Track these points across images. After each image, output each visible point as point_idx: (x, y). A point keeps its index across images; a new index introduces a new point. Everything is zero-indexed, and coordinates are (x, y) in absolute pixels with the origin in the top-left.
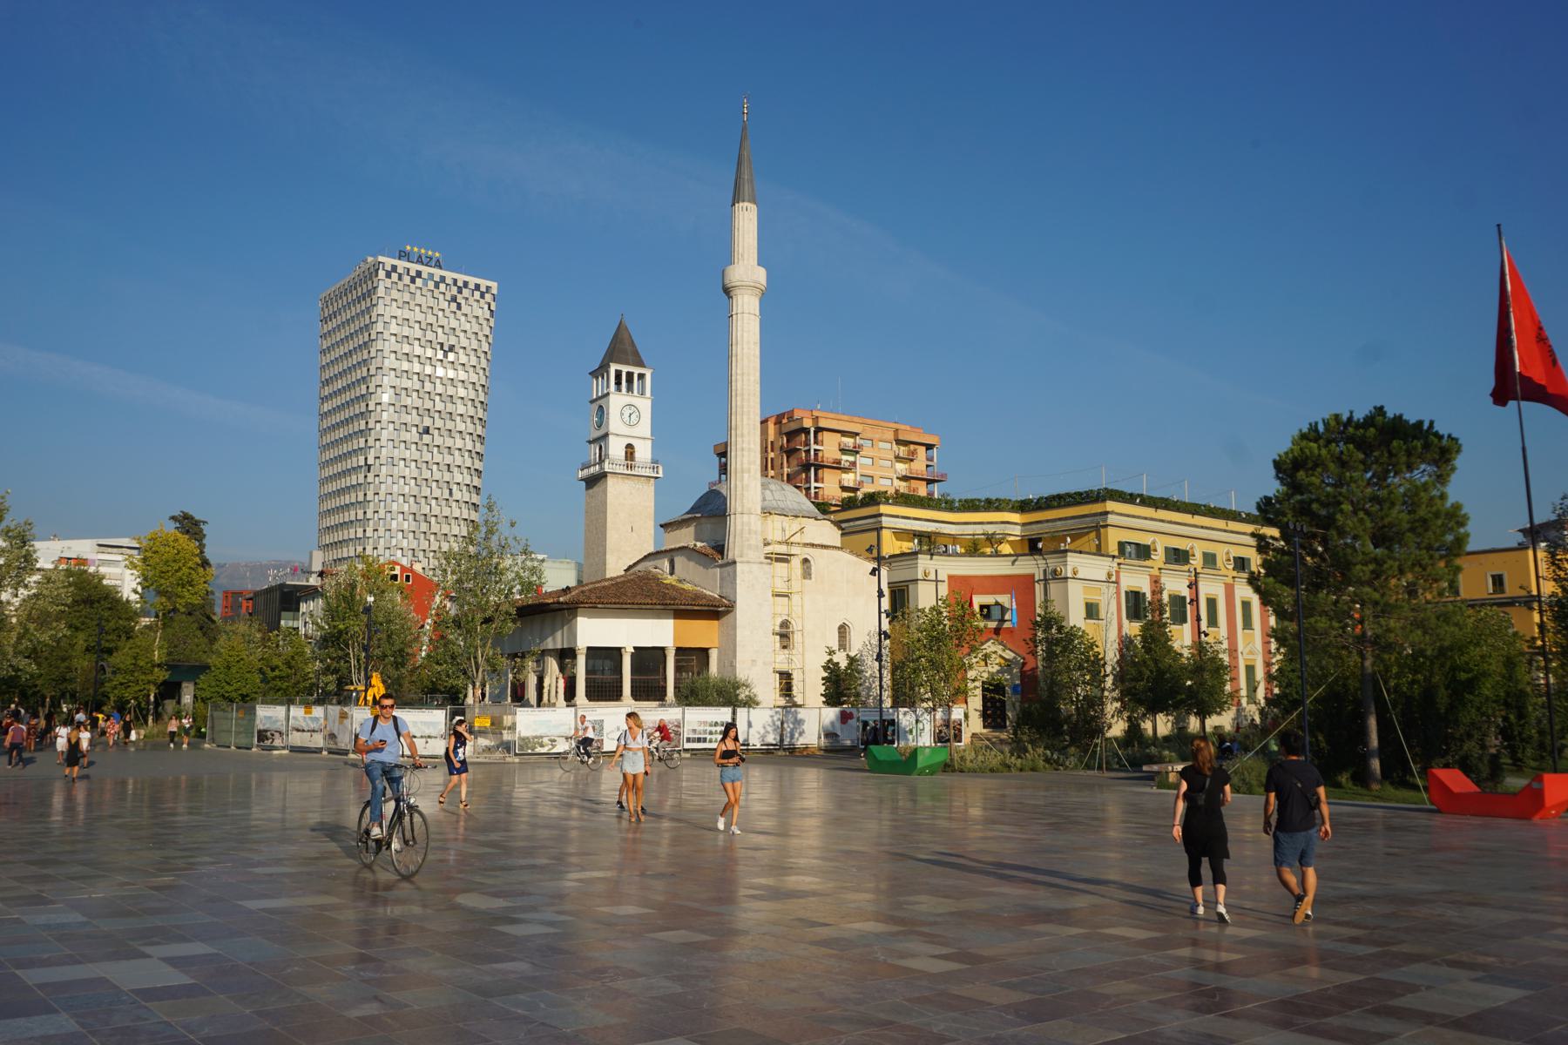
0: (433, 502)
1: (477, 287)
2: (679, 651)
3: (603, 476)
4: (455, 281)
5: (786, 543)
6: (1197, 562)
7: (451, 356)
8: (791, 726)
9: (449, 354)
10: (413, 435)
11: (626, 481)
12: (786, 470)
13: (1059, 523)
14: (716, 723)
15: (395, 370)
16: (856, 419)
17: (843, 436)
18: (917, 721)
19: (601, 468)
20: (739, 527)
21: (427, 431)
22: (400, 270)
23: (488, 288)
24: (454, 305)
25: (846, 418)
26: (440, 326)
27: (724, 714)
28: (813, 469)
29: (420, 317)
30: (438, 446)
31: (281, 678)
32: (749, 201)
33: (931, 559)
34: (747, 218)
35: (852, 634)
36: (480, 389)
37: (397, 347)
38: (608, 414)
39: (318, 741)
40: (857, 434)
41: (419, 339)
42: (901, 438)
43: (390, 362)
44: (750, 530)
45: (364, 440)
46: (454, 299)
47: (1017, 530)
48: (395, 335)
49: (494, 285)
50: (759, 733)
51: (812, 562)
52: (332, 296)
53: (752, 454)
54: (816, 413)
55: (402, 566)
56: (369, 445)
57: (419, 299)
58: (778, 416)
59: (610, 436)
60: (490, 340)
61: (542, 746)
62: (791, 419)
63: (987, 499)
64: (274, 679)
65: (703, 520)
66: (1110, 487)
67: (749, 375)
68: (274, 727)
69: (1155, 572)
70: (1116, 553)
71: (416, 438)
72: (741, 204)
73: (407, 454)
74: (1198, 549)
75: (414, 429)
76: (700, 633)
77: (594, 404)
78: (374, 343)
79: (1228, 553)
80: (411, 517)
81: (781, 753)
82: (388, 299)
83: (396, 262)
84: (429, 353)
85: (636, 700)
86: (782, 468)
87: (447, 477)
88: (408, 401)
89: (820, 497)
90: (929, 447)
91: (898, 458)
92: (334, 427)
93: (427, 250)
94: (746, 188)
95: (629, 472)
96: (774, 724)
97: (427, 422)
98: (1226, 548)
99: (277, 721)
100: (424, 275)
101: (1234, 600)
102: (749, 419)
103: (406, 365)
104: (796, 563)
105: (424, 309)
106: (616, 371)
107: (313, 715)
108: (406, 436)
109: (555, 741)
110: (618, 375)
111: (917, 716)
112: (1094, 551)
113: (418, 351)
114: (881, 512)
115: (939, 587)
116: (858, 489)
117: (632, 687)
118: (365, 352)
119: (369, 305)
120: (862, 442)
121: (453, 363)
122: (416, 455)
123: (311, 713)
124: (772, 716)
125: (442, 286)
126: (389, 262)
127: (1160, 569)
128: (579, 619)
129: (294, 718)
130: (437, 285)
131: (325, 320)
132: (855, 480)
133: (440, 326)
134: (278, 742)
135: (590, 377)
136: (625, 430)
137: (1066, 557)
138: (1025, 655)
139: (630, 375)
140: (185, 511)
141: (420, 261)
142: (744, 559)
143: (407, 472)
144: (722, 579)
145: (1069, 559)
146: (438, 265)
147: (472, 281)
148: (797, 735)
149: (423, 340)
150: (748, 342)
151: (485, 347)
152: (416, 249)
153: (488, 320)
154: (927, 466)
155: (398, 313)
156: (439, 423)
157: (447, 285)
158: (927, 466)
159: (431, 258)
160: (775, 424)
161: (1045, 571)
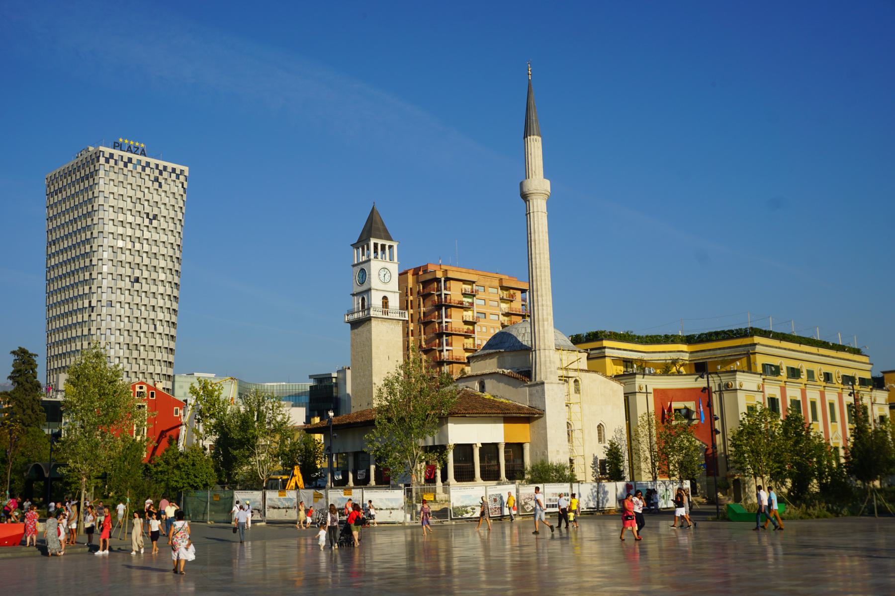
0: (142, 335)
1: (174, 170)
2: (508, 445)
3: (368, 319)
4: (157, 166)
5: (566, 369)
6: (804, 376)
12: (422, 309)
13: (719, 351)
15: (113, 233)
16: (471, 271)
17: (464, 284)
18: (666, 490)
19: (369, 314)
21: (137, 280)
22: (116, 157)
23: (182, 171)
24: (156, 184)
25: (464, 270)
27: (565, 488)
28: (444, 308)
29: (131, 193)
30: (146, 292)
31: (161, 472)
32: (537, 135)
33: (643, 378)
34: (535, 145)
35: (605, 431)
36: (176, 248)
37: (113, 216)
38: (370, 275)
40: (474, 282)
41: (131, 210)
42: (504, 284)
43: (110, 228)
44: (550, 360)
45: (88, 287)
46: (157, 179)
47: (686, 357)
48: (113, 207)
49: (186, 169)
51: (580, 382)
53: (549, 308)
54: (444, 267)
55: (148, 386)
56: (93, 291)
57: (131, 179)
58: (415, 269)
59: (372, 291)
60: (184, 211)
61: (467, 513)
62: (425, 272)
63: (666, 335)
64: (156, 473)
65: (505, 354)
66: (754, 327)
67: (544, 253)
69: (782, 384)
70: (761, 372)
71: (129, 285)
72: (532, 137)
73: (122, 298)
74: (805, 367)
75: (128, 279)
76: (521, 433)
77: (355, 268)
78: (96, 213)
79: (820, 370)
80: (125, 347)
81: (598, 514)
84: (139, 220)
85: (484, 481)
86: (419, 307)
88: (122, 258)
89: (449, 328)
90: (523, 291)
91: (502, 300)
93: (135, 142)
94: (534, 126)
95: (386, 317)
97: (137, 273)
98: (819, 366)
99: (256, 502)
100: (134, 161)
101: (825, 401)
102: (545, 284)
103: (121, 230)
104: (571, 381)
105: (134, 187)
106: (374, 243)
107: (287, 497)
108: (121, 284)
109: (474, 509)
110: (376, 245)
111: (666, 486)
112: (746, 369)
113: (130, 219)
114: (604, 346)
116: (475, 323)
117: (481, 471)
118: (89, 220)
119: (91, 183)
120: (477, 288)
121: (156, 228)
122: (129, 299)
123: (285, 495)
124: (592, 490)
125: (148, 169)
126: (108, 151)
127: (785, 382)
129: (270, 499)
130: (144, 169)
131: (50, 195)
132: (473, 317)
133: (146, 200)
135: (352, 247)
136: (381, 286)
137: (735, 375)
138: (707, 443)
139: (383, 247)
140: (23, 347)
141: (129, 150)
143: (122, 312)
144: (531, 395)
145: (737, 376)
146: (143, 153)
147: (170, 165)
148: (605, 501)
149: (134, 211)
151: (180, 216)
152: (126, 141)
153: (182, 195)
154: (522, 305)
155: (115, 190)
156: (146, 274)
157: (151, 168)
158: (522, 305)
159: (138, 148)
160: (413, 275)
161: (719, 385)
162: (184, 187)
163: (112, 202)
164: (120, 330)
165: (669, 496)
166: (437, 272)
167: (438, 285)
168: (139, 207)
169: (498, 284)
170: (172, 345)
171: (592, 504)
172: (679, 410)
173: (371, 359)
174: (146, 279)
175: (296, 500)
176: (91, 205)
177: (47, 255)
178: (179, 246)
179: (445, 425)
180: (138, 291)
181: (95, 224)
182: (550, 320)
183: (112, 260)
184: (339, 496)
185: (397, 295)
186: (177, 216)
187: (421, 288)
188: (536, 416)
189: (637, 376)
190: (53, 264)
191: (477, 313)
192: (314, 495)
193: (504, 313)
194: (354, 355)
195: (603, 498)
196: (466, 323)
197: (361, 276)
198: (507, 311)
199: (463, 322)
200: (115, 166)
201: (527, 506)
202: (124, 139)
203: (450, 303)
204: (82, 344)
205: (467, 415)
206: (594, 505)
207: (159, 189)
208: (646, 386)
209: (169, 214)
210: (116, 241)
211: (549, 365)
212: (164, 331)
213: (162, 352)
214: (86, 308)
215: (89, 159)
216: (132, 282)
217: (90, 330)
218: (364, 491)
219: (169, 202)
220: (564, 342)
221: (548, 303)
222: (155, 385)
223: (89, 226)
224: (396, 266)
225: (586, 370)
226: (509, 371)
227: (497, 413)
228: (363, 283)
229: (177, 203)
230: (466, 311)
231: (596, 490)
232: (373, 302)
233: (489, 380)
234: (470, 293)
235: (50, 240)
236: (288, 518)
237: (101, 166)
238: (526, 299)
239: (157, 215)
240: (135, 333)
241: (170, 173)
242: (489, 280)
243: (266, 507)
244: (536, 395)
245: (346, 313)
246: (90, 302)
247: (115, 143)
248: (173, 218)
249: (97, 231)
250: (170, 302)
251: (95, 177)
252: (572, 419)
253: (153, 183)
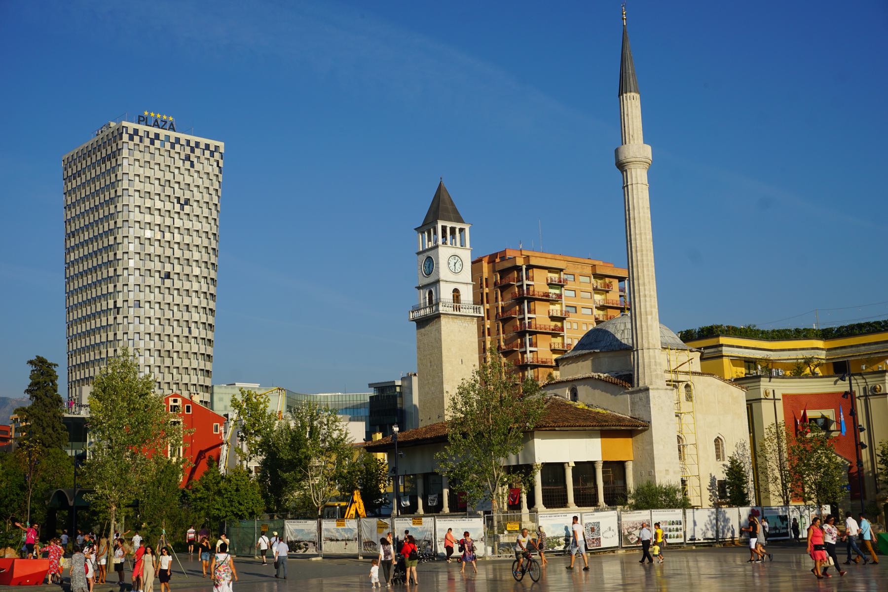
0: (175, 340)
1: (207, 147)
2: (606, 463)
3: (438, 316)
4: (188, 142)
5: (675, 372)
7: (187, 209)
8: (722, 524)
9: (185, 206)
10: (156, 280)
11: (455, 321)
13: (863, 348)
14: (673, 522)
15: (139, 222)
16: (558, 257)
17: (550, 272)
19: (437, 310)
20: (646, 361)
21: (168, 276)
22: (141, 133)
23: (217, 147)
24: (188, 164)
25: (549, 256)
26: (176, 182)
28: (526, 302)
29: (159, 174)
30: (178, 289)
31: (200, 498)
32: (636, 92)
33: (770, 381)
34: (633, 105)
35: (724, 446)
36: (212, 237)
37: (139, 202)
38: (438, 264)
39: (353, 548)
40: (561, 270)
41: (159, 195)
42: (598, 272)
43: (136, 215)
44: (655, 362)
46: (188, 158)
47: (823, 355)
48: (139, 191)
49: (221, 144)
50: (702, 530)
52: (75, 157)
54: (525, 253)
57: (159, 159)
59: (441, 283)
60: (220, 194)
61: (559, 545)
62: (503, 258)
64: (195, 500)
65: (601, 355)
67: (645, 234)
68: (306, 538)
72: (628, 94)
73: (151, 297)
75: (157, 275)
77: (421, 256)
78: (120, 199)
80: (156, 353)
81: (718, 546)
82: (131, 159)
83: (137, 126)
84: (169, 206)
85: (579, 506)
87: (186, 316)
88: (151, 250)
89: (533, 326)
90: (621, 279)
91: (596, 290)
92: (81, 274)
93: (162, 115)
95: (458, 313)
96: (711, 523)
97: (168, 268)
99: (312, 533)
100: (162, 137)
102: (648, 270)
103: (148, 218)
104: (682, 386)
105: (163, 167)
106: (442, 226)
107: (346, 527)
108: (150, 281)
110: (444, 229)
111: (800, 512)
113: (159, 205)
115: (776, 404)
116: (564, 319)
118: (112, 207)
119: (114, 164)
120: (566, 277)
121: (188, 215)
122: (159, 298)
124: (709, 516)
125: (177, 147)
126: (131, 126)
128: (536, 440)
129: (326, 530)
130: (173, 147)
131: (68, 179)
132: (561, 311)
133: (176, 182)
134: (312, 550)
135: (416, 232)
136: (452, 277)
138: (851, 459)
139: (453, 230)
140: (40, 356)
141: (156, 124)
142: (655, 387)
143: (151, 313)
146: (172, 128)
147: (203, 141)
149: (162, 195)
150: (644, 207)
151: (215, 200)
152: (152, 114)
153: (217, 176)
154: (620, 296)
155: (141, 171)
156: (178, 269)
157: (182, 145)
158: (620, 296)
159: (166, 122)
160: (488, 263)
161: (865, 389)
162: (220, 166)
163: (138, 185)
164: (150, 334)
165: (805, 524)
166: (517, 258)
167: (518, 274)
168: (168, 191)
169: (591, 272)
170: (210, 351)
171: (710, 535)
172: (815, 420)
173: (441, 364)
174: (178, 274)
175: (356, 531)
176: (114, 190)
177: (66, 249)
178: (214, 234)
179: (531, 442)
180: (169, 288)
181: (118, 212)
182: (654, 314)
183: (139, 253)
184: (409, 527)
185: (471, 287)
186: (212, 199)
187: (499, 278)
188: (639, 428)
189: (762, 379)
190: (72, 259)
191: (566, 306)
192: (378, 524)
193: (598, 306)
194: (420, 359)
195: (724, 527)
196: (553, 318)
197: (427, 266)
198: (601, 304)
199: (550, 317)
200: (140, 144)
201: (631, 537)
202: (150, 112)
203: (534, 295)
204: (107, 351)
205: (557, 429)
206: (712, 535)
207: (191, 169)
208: (774, 391)
209: (203, 199)
210: (143, 230)
211: (654, 367)
212: (199, 334)
213: (198, 360)
214: (111, 309)
215: (110, 137)
216: (162, 278)
217: (115, 334)
218: (437, 520)
219: (203, 184)
220: (672, 339)
221: (652, 293)
222: (191, 398)
223: (112, 214)
224: (469, 252)
225: (700, 373)
226: (605, 375)
227: (593, 426)
228: (430, 274)
229: (212, 185)
230: (552, 304)
231: (715, 517)
232: (442, 296)
233: (582, 386)
234: (557, 283)
235: (69, 232)
236: (348, 552)
237: (125, 145)
238: (625, 288)
239: (189, 199)
240: (167, 338)
241: (204, 150)
242: (580, 266)
243: (323, 539)
244: (640, 403)
245: (411, 309)
246: (115, 302)
247: (139, 116)
248: (207, 203)
249: (122, 220)
250: (206, 300)
251: (118, 157)
252: (684, 432)
253: (184, 163)
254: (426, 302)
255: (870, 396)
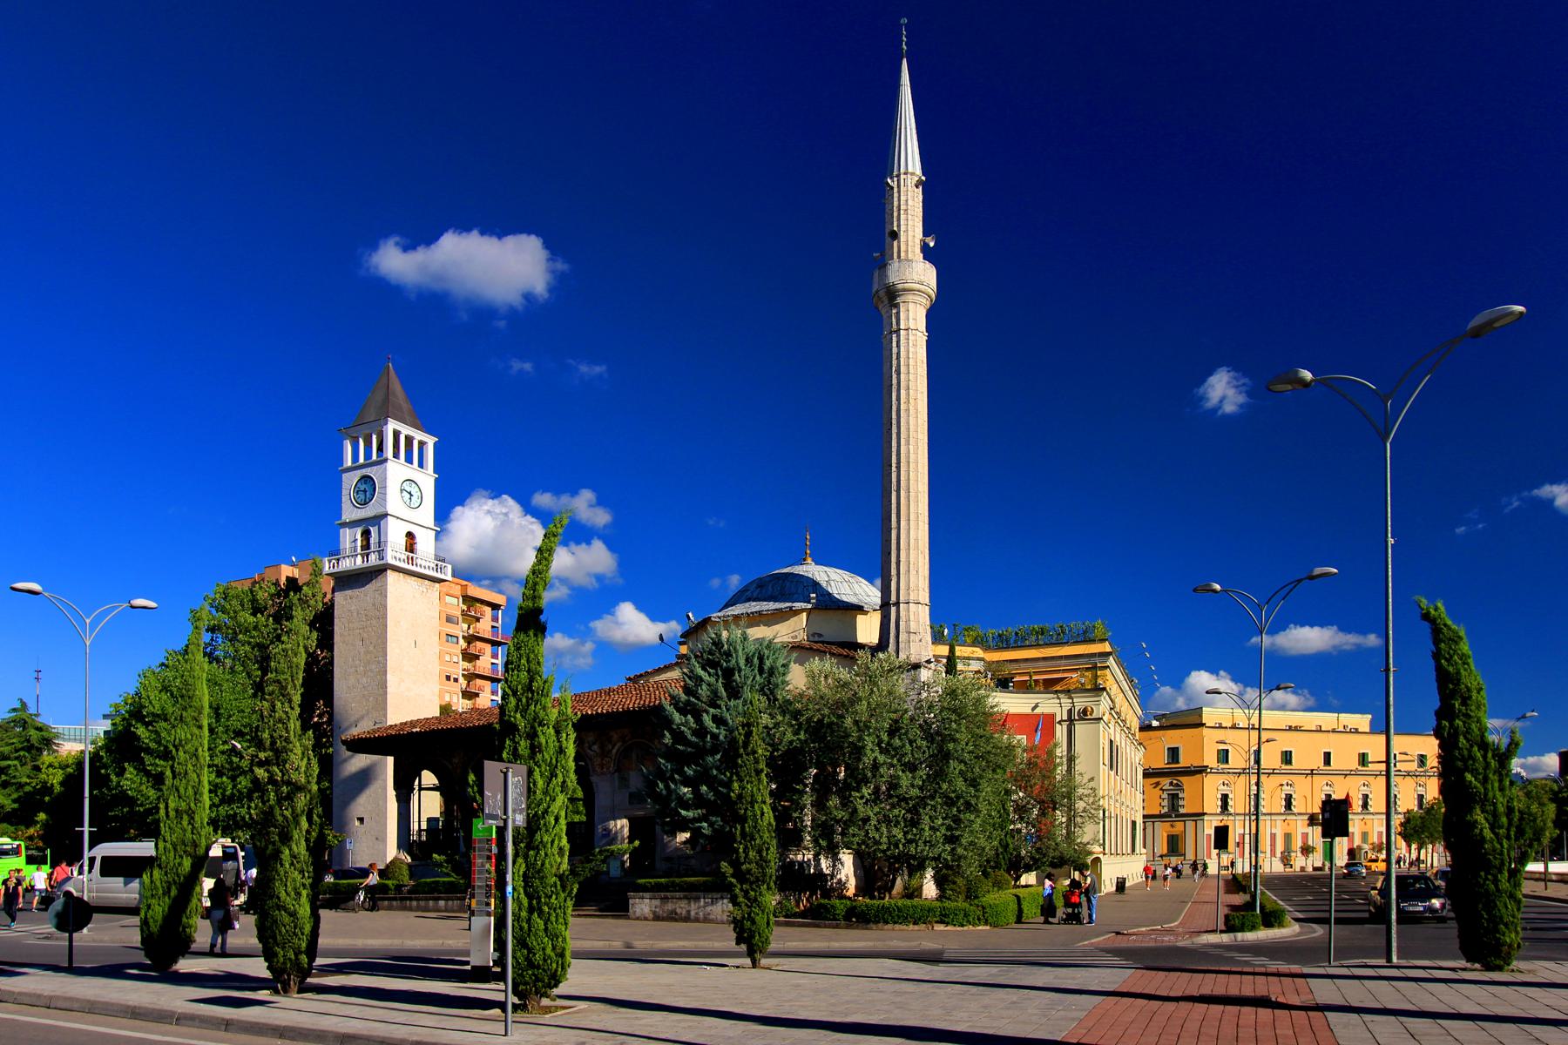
3: (380, 571)
90: (495, 607)
110: (396, 434)
154: (493, 627)
158: (493, 627)
161: (1070, 712)
169: (460, 593)
232: (390, 538)
254: (355, 547)
255: (1076, 720)
